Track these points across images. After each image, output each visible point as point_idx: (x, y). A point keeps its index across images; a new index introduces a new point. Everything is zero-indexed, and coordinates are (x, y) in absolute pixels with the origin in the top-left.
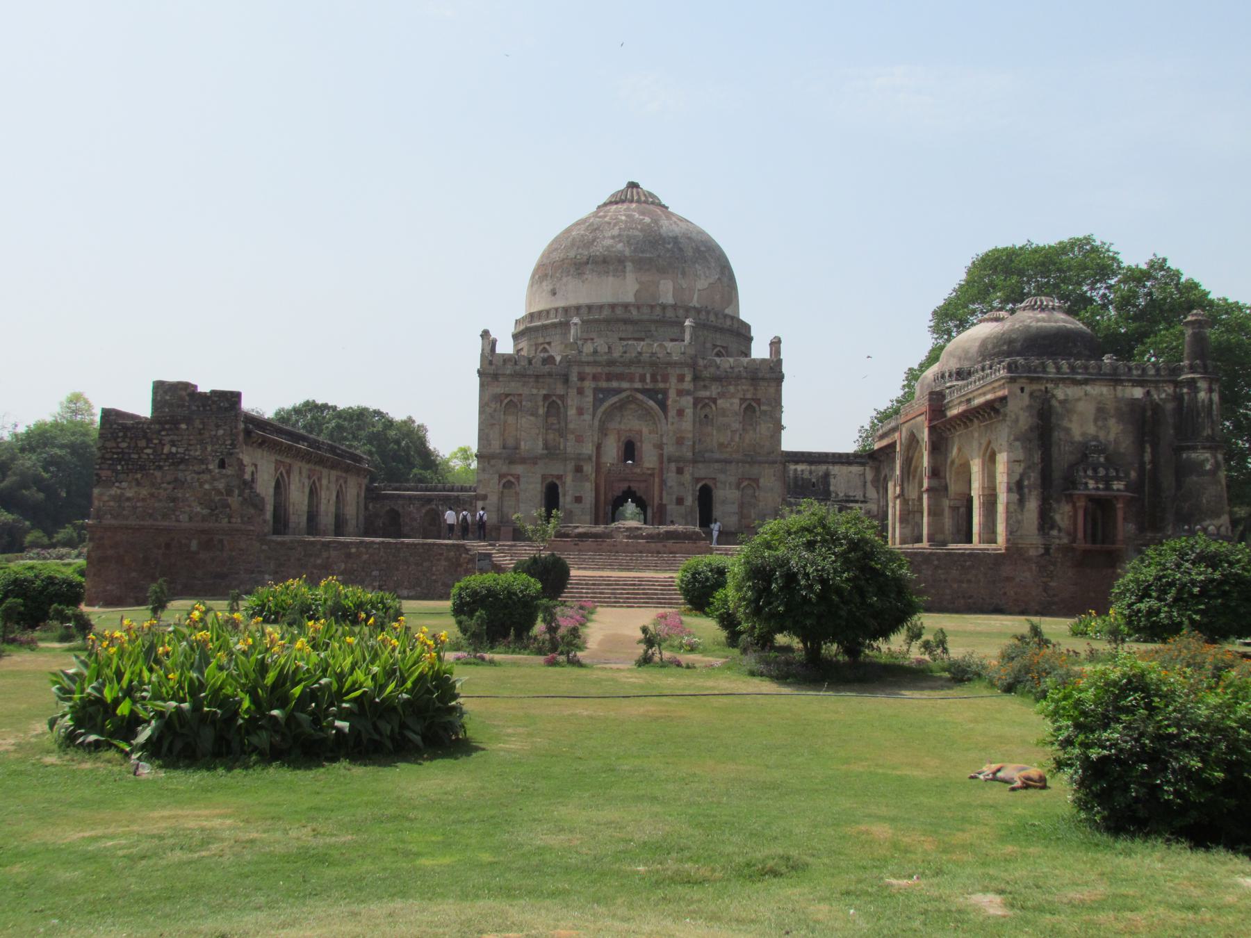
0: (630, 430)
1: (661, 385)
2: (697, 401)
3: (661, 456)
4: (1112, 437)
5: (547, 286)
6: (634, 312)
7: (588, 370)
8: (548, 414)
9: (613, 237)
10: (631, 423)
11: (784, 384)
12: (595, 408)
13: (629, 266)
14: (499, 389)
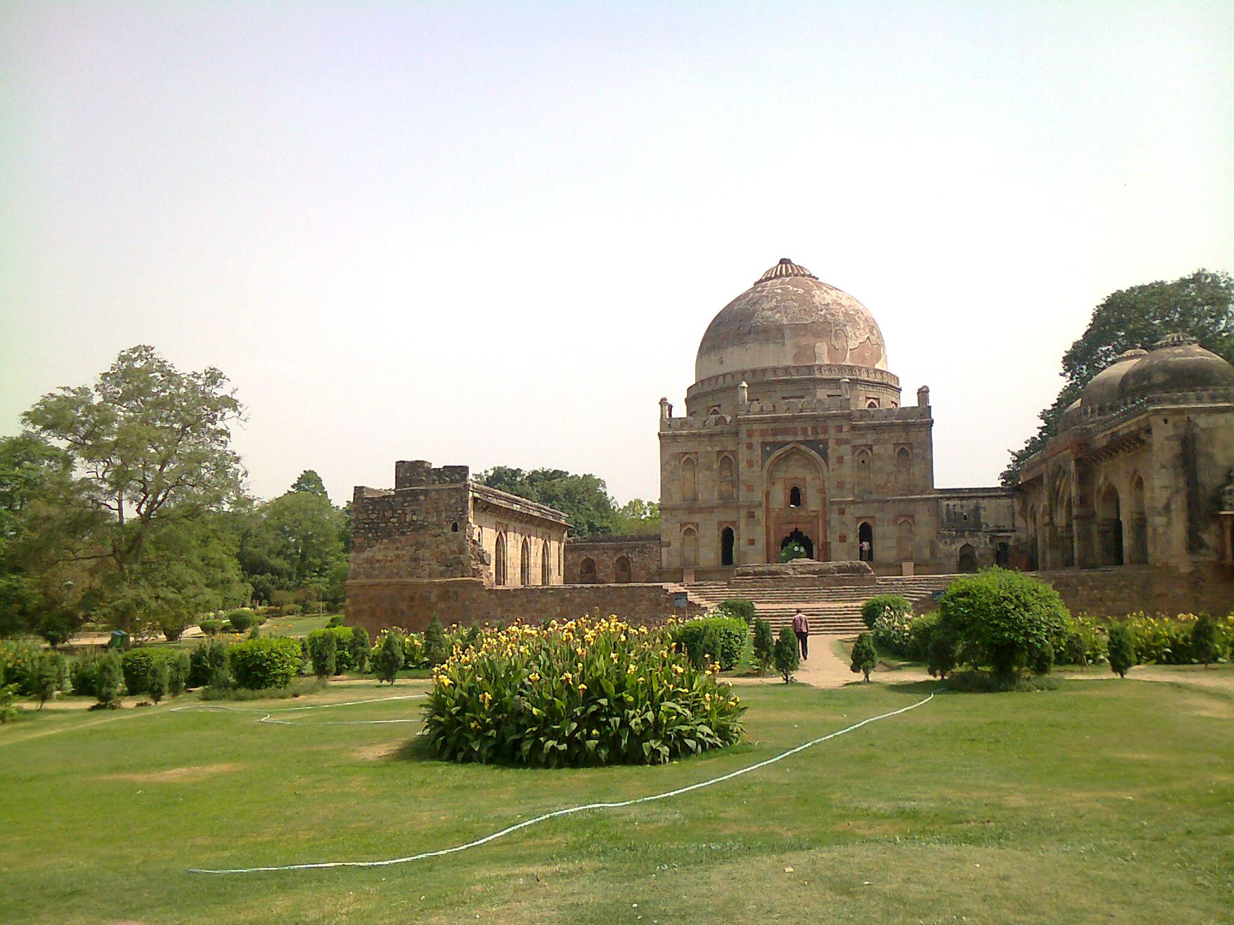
1: (821, 437)
7: (755, 427)
8: (721, 468)
9: (770, 309)
10: (796, 472)
12: (763, 461)
14: (676, 449)
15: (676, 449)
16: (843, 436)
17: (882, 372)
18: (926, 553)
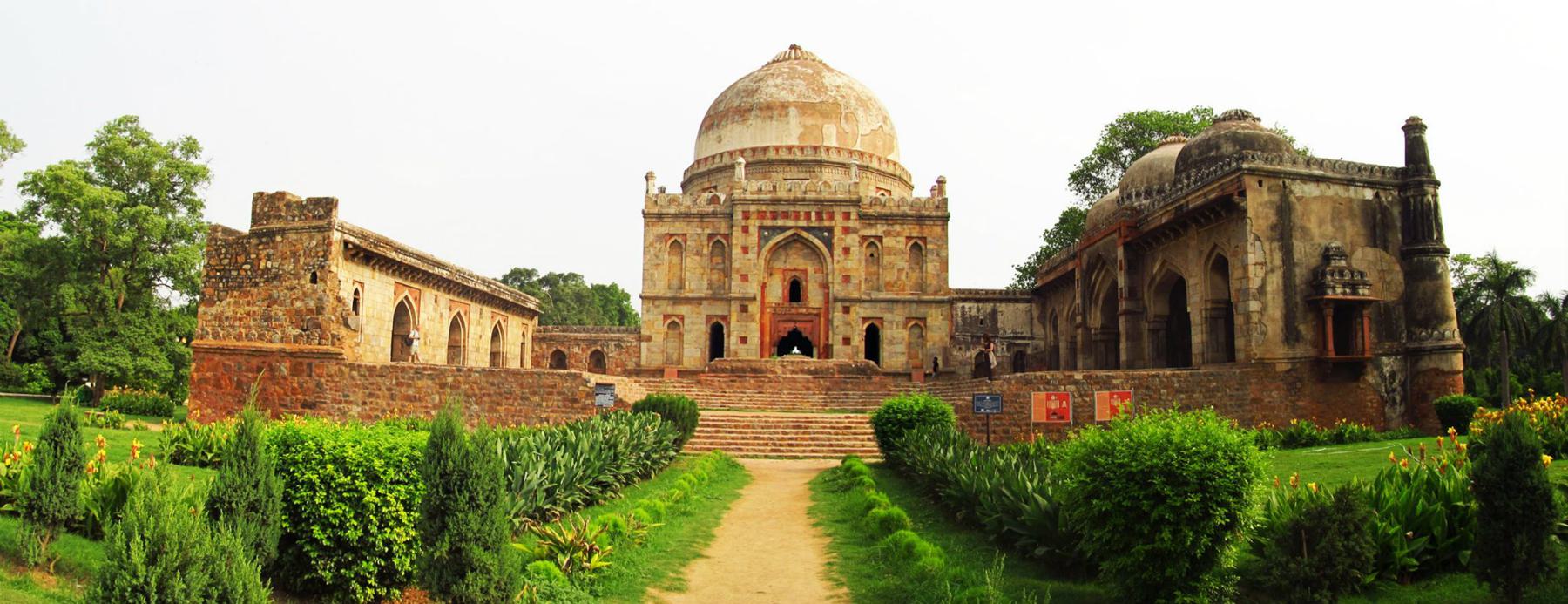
1: (826, 223)
4: (1348, 239)
5: (713, 135)
7: (753, 208)
8: (712, 255)
10: (796, 261)
12: (760, 247)
13: (793, 111)
14: (663, 229)
15: (663, 229)
16: (852, 223)
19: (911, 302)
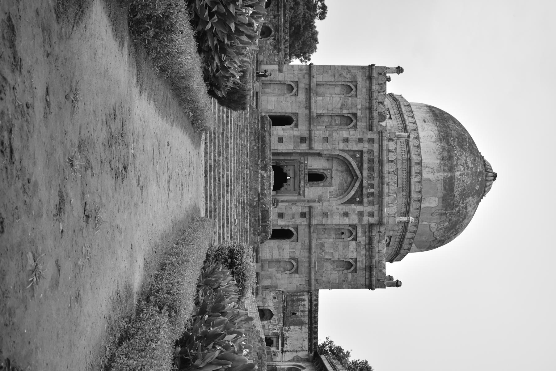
0: (332, 177)
1: (365, 200)
2: (355, 227)
3: (315, 202)
5: (428, 116)
6: (417, 179)
7: (376, 146)
8: (342, 116)
9: (466, 163)
10: (338, 178)
11: (367, 290)
17: (409, 250)
18: (267, 283)
19: (310, 262)
